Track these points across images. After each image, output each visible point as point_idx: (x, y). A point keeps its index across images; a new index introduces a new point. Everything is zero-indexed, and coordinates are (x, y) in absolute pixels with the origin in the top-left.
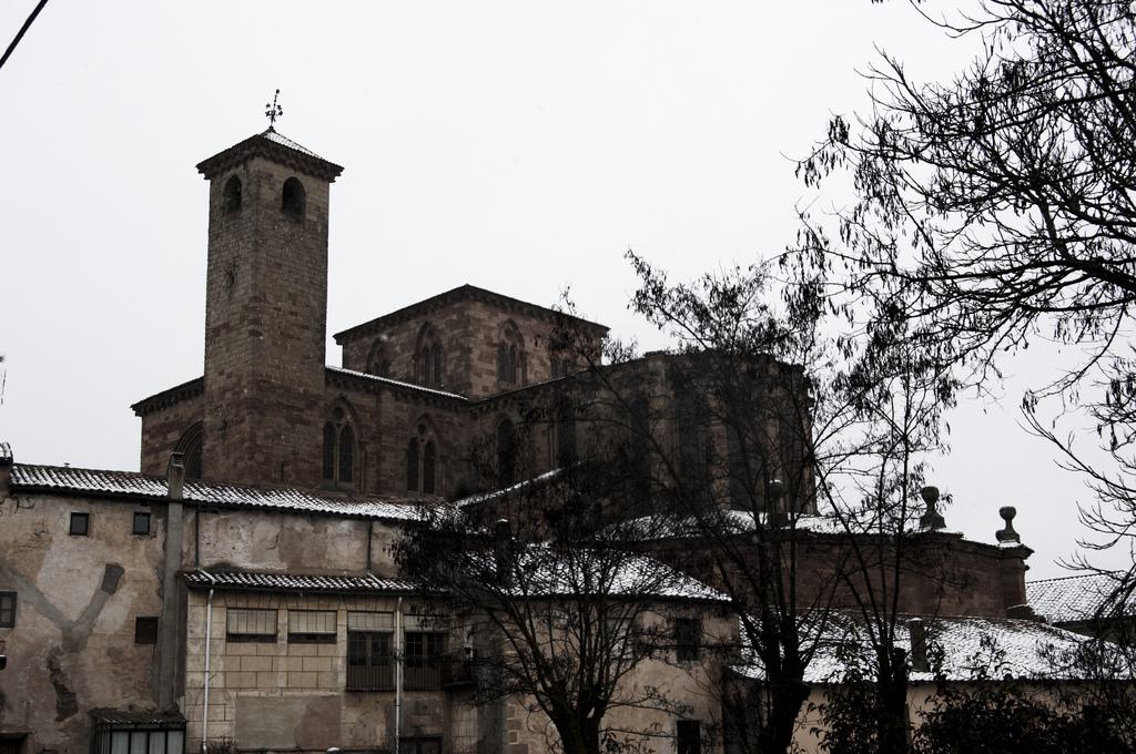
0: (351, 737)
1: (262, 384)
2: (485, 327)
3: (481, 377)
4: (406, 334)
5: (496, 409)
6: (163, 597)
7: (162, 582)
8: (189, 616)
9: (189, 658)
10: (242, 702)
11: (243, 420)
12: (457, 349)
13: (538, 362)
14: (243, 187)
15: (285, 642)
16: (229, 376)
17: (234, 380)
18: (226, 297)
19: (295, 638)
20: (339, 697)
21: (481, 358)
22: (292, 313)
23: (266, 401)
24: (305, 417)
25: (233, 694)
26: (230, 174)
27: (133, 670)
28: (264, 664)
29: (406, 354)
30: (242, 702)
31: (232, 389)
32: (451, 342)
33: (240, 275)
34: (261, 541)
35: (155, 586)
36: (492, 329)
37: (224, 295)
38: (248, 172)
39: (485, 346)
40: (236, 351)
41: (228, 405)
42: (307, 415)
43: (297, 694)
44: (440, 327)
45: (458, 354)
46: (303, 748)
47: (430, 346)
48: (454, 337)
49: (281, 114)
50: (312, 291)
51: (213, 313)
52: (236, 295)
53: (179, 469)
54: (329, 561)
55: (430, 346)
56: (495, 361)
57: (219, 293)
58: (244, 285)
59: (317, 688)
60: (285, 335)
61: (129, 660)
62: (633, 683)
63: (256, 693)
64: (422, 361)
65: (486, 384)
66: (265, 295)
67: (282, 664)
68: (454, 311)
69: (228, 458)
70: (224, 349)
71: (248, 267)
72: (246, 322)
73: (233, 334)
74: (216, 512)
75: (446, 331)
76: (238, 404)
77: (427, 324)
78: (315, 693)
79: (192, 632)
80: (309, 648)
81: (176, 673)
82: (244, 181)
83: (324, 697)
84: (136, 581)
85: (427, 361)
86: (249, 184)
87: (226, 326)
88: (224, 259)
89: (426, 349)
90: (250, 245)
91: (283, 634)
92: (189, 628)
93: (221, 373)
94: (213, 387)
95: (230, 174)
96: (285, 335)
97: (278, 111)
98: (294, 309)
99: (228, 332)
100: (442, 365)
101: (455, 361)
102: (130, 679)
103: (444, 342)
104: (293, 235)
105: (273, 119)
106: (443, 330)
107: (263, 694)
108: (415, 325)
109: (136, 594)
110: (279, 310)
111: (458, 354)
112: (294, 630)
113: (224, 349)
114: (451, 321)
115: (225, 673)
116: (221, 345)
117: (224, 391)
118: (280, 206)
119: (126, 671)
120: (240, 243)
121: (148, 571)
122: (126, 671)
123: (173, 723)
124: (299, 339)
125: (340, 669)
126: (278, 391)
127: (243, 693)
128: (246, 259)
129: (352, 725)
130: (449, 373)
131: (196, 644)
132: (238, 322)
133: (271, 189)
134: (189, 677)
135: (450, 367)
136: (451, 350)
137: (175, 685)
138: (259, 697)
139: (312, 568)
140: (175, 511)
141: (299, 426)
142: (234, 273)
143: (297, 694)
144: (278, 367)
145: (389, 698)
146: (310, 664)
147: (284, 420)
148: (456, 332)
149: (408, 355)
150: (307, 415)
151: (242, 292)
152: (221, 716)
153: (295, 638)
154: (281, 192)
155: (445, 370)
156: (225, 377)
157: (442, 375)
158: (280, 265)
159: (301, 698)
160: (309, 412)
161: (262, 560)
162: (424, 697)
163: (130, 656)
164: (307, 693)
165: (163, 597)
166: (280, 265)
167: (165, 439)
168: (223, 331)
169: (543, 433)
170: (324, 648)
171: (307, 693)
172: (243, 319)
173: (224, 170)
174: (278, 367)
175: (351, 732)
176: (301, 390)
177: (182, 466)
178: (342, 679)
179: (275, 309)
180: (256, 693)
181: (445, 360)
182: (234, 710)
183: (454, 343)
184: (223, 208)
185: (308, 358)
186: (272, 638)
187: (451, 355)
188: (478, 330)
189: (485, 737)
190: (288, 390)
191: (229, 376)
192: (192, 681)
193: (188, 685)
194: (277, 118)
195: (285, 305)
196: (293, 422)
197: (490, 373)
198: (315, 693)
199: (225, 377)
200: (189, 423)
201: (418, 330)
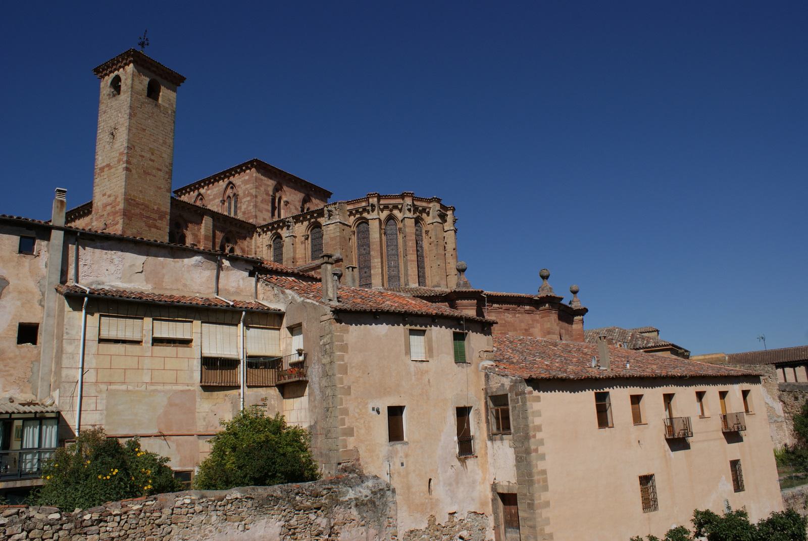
0: (204, 424)
1: (130, 201)
2: (266, 185)
3: (262, 212)
4: (217, 189)
5: (271, 231)
6: (43, 306)
7: (43, 294)
8: (66, 320)
9: (64, 356)
10: (111, 394)
11: (117, 224)
12: (248, 196)
13: (294, 208)
14: (122, 81)
15: (150, 345)
16: (109, 196)
17: (112, 198)
18: (109, 149)
19: (157, 341)
20: (194, 391)
21: (262, 201)
22: (153, 161)
23: (133, 211)
24: (157, 224)
25: (103, 387)
26: (112, 75)
27: (14, 368)
28: (132, 362)
30: (111, 394)
31: (111, 204)
32: (244, 193)
33: (118, 134)
34: (130, 266)
35: (38, 296)
36: (268, 186)
38: (126, 72)
39: (265, 195)
40: (114, 180)
41: (108, 214)
42: (159, 223)
43: (159, 388)
44: (238, 184)
45: (249, 198)
46: (165, 433)
47: (231, 195)
49: (148, 44)
50: (165, 149)
52: (116, 146)
53: (62, 202)
54: (185, 285)
55: (231, 195)
56: (270, 204)
57: (104, 146)
58: (121, 140)
59: (176, 383)
60: (146, 173)
61: (10, 359)
62: (427, 380)
63: (124, 387)
64: (226, 204)
65: (265, 217)
66: (134, 147)
67: (147, 363)
70: (107, 180)
71: (124, 129)
72: (122, 162)
73: (113, 170)
74: (93, 240)
75: (242, 186)
76: (115, 213)
77: (230, 183)
78: (175, 388)
79: (67, 333)
80: (169, 350)
81: (53, 370)
82: (123, 78)
83: (182, 391)
84: (20, 292)
85: (230, 204)
86: (126, 79)
87: (108, 166)
88: (109, 125)
89: (229, 197)
90: (126, 116)
91: (148, 340)
92: (65, 330)
93: (104, 195)
94: (99, 204)
96: (146, 173)
97: (146, 43)
98: (153, 158)
99: (109, 169)
100: (239, 205)
101: (247, 203)
102: (11, 375)
103: (241, 193)
104: (153, 113)
105: (143, 47)
106: (239, 185)
107: (130, 388)
108: (222, 184)
109: (19, 303)
110: (143, 156)
111: (249, 198)
112: (157, 335)
113: (107, 180)
114: (245, 180)
115: (97, 369)
116: (105, 177)
117: (105, 206)
118: (146, 94)
119: (7, 368)
120: (119, 115)
121: (31, 285)
122: (7, 368)
123: (47, 412)
124: (155, 176)
125: (195, 368)
126: (140, 206)
127: (113, 387)
128: (123, 124)
129: (204, 414)
130: (243, 210)
131: (71, 344)
132: (116, 163)
133: (140, 83)
134: (64, 372)
135: (244, 207)
136: (245, 196)
137: (52, 381)
138: (128, 391)
139: (171, 289)
140: (57, 237)
141: (153, 230)
142: (114, 133)
143: (159, 388)
144: (141, 191)
145: (234, 392)
146: (171, 364)
147: (144, 224)
148: (248, 186)
149: (218, 201)
150: (159, 223)
151: (120, 144)
152: (93, 407)
153: (157, 341)
154: (147, 86)
155: (241, 207)
156: (106, 197)
157: (238, 211)
158: (144, 130)
159: (163, 391)
160: (160, 221)
161: (130, 281)
162: (262, 392)
163: (11, 355)
164: (168, 387)
165: (43, 306)
166: (144, 130)
168: (106, 169)
169: (302, 243)
170: (181, 350)
171: (168, 387)
172: (119, 161)
173: (111, 72)
174: (141, 191)
175: (204, 419)
176: (155, 208)
177: (65, 200)
178: (197, 376)
179: (140, 156)
180: (124, 387)
181: (241, 202)
182: (104, 401)
183: (246, 193)
184: (110, 95)
185: (160, 188)
186: (138, 342)
187: (245, 200)
188: (261, 186)
189: (316, 423)
190: (148, 207)
191: (109, 196)
192: (66, 377)
193: (63, 379)
194: (146, 46)
195: (147, 155)
196: (149, 227)
197: (267, 211)
198: (175, 388)
199: (106, 197)
201: (224, 186)
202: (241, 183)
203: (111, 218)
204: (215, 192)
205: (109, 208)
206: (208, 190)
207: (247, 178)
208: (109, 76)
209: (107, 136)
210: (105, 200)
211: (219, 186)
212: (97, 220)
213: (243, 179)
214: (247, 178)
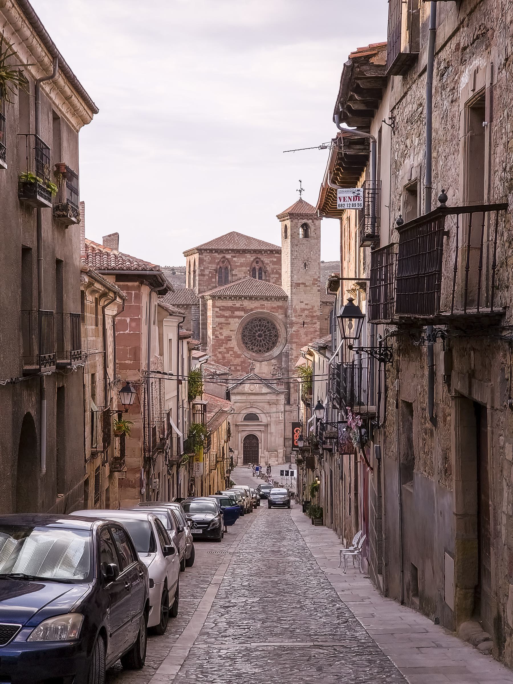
4: (244, 259)
29: (244, 268)
32: (273, 271)
37: (302, 271)
44: (266, 262)
48: (275, 268)
51: (295, 276)
68: (275, 257)
69: (307, 336)
73: (308, 288)
93: (302, 302)
95: (304, 221)
106: (267, 264)
114: (272, 260)
136: (273, 273)
167: (234, 313)
172: (314, 284)
181: (270, 277)
183: (275, 271)
191: (307, 304)
200: (252, 310)
201: (252, 259)
202: (269, 262)
203: (310, 319)
204: (242, 262)
205: (306, 312)
206: (234, 257)
207: (275, 260)
208: (298, 220)
209: (301, 264)
210: (303, 306)
211: (246, 257)
212: (295, 316)
213: (271, 259)
214: (275, 260)
